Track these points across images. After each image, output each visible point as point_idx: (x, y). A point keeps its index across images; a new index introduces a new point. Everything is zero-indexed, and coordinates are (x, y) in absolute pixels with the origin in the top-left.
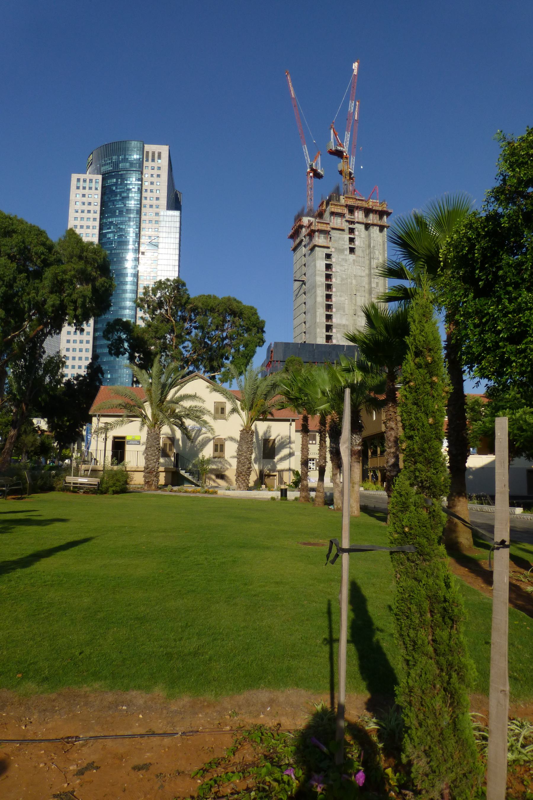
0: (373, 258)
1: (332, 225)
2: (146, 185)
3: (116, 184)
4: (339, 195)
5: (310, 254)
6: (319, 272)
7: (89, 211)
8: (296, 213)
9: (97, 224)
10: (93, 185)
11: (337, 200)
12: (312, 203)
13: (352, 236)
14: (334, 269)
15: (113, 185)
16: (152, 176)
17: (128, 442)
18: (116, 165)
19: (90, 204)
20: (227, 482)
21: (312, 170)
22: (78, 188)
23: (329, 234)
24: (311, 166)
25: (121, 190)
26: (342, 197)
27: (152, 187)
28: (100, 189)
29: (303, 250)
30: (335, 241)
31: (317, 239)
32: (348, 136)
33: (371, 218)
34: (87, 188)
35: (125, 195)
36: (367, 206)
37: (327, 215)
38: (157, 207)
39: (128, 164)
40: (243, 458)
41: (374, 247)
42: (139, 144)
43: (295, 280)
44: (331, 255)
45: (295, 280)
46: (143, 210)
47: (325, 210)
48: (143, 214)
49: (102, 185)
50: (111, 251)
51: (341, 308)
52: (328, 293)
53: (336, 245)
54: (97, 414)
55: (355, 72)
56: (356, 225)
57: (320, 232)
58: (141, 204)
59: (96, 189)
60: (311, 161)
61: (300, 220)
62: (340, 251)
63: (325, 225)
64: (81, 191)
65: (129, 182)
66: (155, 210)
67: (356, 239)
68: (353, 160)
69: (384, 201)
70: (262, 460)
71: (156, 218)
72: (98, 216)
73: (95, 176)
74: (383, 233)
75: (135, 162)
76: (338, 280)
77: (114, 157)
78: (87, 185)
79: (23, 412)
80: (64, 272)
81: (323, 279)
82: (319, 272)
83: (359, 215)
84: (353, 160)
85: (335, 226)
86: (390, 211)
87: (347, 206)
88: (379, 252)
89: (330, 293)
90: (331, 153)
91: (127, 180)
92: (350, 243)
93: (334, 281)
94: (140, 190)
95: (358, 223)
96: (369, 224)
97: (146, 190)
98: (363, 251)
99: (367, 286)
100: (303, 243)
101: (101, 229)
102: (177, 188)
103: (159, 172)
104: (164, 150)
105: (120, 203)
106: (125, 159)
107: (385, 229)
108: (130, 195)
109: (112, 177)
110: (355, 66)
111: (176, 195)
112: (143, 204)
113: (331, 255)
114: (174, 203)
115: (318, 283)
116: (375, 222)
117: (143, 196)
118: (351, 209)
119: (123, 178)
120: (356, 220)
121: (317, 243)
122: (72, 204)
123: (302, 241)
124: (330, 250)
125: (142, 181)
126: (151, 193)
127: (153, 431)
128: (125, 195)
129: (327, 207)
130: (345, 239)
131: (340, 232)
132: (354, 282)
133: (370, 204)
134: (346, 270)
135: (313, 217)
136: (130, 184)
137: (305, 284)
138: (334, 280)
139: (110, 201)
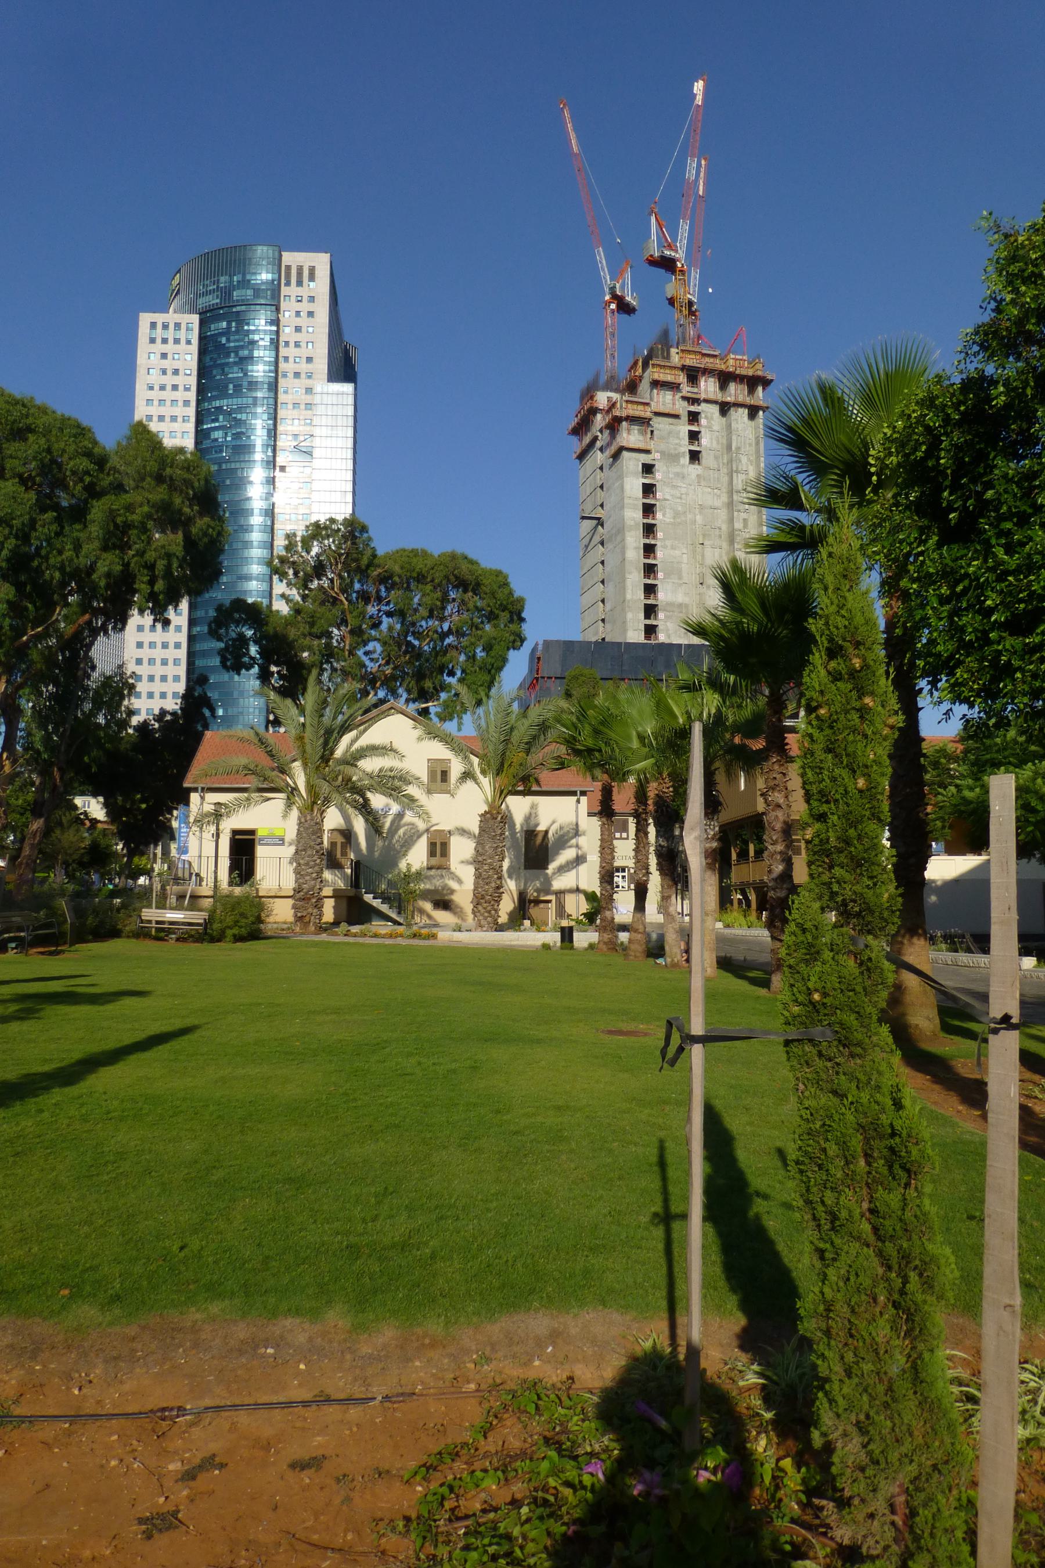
0: (737, 472)
1: (654, 407)
2: (287, 332)
3: (227, 332)
4: (669, 347)
5: (611, 466)
6: (631, 501)
7: (175, 387)
8: (583, 384)
9: (191, 411)
10: (182, 335)
11: (663, 357)
12: (614, 364)
13: (694, 428)
14: (659, 495)
15: (222, 334)
16: (298, 314)
17: (260, 840)
18: (226, 293)
19: (176, 372)
20: (455, 913)
21: (615, 297)
22: (152, 341)
23: (649, 425)
24: (612, 290)
25: (237, 344)
26: (673, 351)
27: (298, 337)
28: (195, 341)
29: (598, 457)
30: (662, 438)
31: (625, 435)
32: (684, 228)
33: (733, 392)
34: (171, 341)
35: (246, 352)
36: (723, 367)
37: (644, 386)
38: (309, 377)
39: (250, 292)
40: (486, 867)
41: (738, 448)
42: (271, 252)
43: (583, 518)
44: (653, 466)
45: (583, 518)
46: (282, 382)
47: (641, 378)
48: (281, 390)
49: (200, 334)
50: (220, 464)
51: (675, 571)
52: (648, 541)
53: (663, 446)
54: (200, 786)
55: (699, 100)
56: (703, 405)
57: (631, 421)
58: (276, 371)
59: (189, 342)
60: (611, 280)
61: (592, 398)
62: (672, 458)
63: (641, 407)
64: (159, 347)
65: (252, 328)
66: (304, 382)
67: (703, 433)
68: (695, 276)
69: (759, 357)
70: (523, 872)
71: (308, 399)
72: (192, 396)
73: (186, 315)
74: (757, 420)
75: (263, 287)
76: (668, 515)
77: (222, 279)
78: (170, 334)
79: (55, 786)
80: (130, 508)
81: (639, 514)
82: (631, 501)
83: (708, 387)
84: (695, 276)
85: (662, 409)
86: (769, 377)
87: (683, 368)
88: (749, 460)
89: (653, 542)
90: (653, 262)
91: (248, 324)
92: (691, 443)
94: (275, 344)
95: (707, 401)
96: (727, 403)
97: (287, 344)
98: (716, 458)
99: (724, 527)
100: (598, 444)
101: (199, 422)
102: (349, 337)
103: (311, 307)
104: (321, 262)
105: (236, 369)
106: (244, 280)
107: (761, 413)
108: (256, 354)
109: (219, 318)
110: (699, 87)
111: (346, 352)
112: (280, 370)
113: (653, 466)
114: (343, 367)
115: (629, 523)
116: (741, 399)
117: (281, 354)
118: (693, 375)
119: (241, 320)
120: (703, 396)
121: (625, 444)
122: (141, 372)
123: (596, 438)
124: (651, 456)
125: (278, 326)
126: (297, 349)
127: (309, 817)
128: (246, 352)
129: (644, 371)
130: (681, 434)
131: (671, 420)
132: (698, 517)
133: (731, 364)
134: (684, 496)
135: (616, 391)
136: (254, 332)
137: (602, 525)
138: (659, 515)
139: (216, 366)
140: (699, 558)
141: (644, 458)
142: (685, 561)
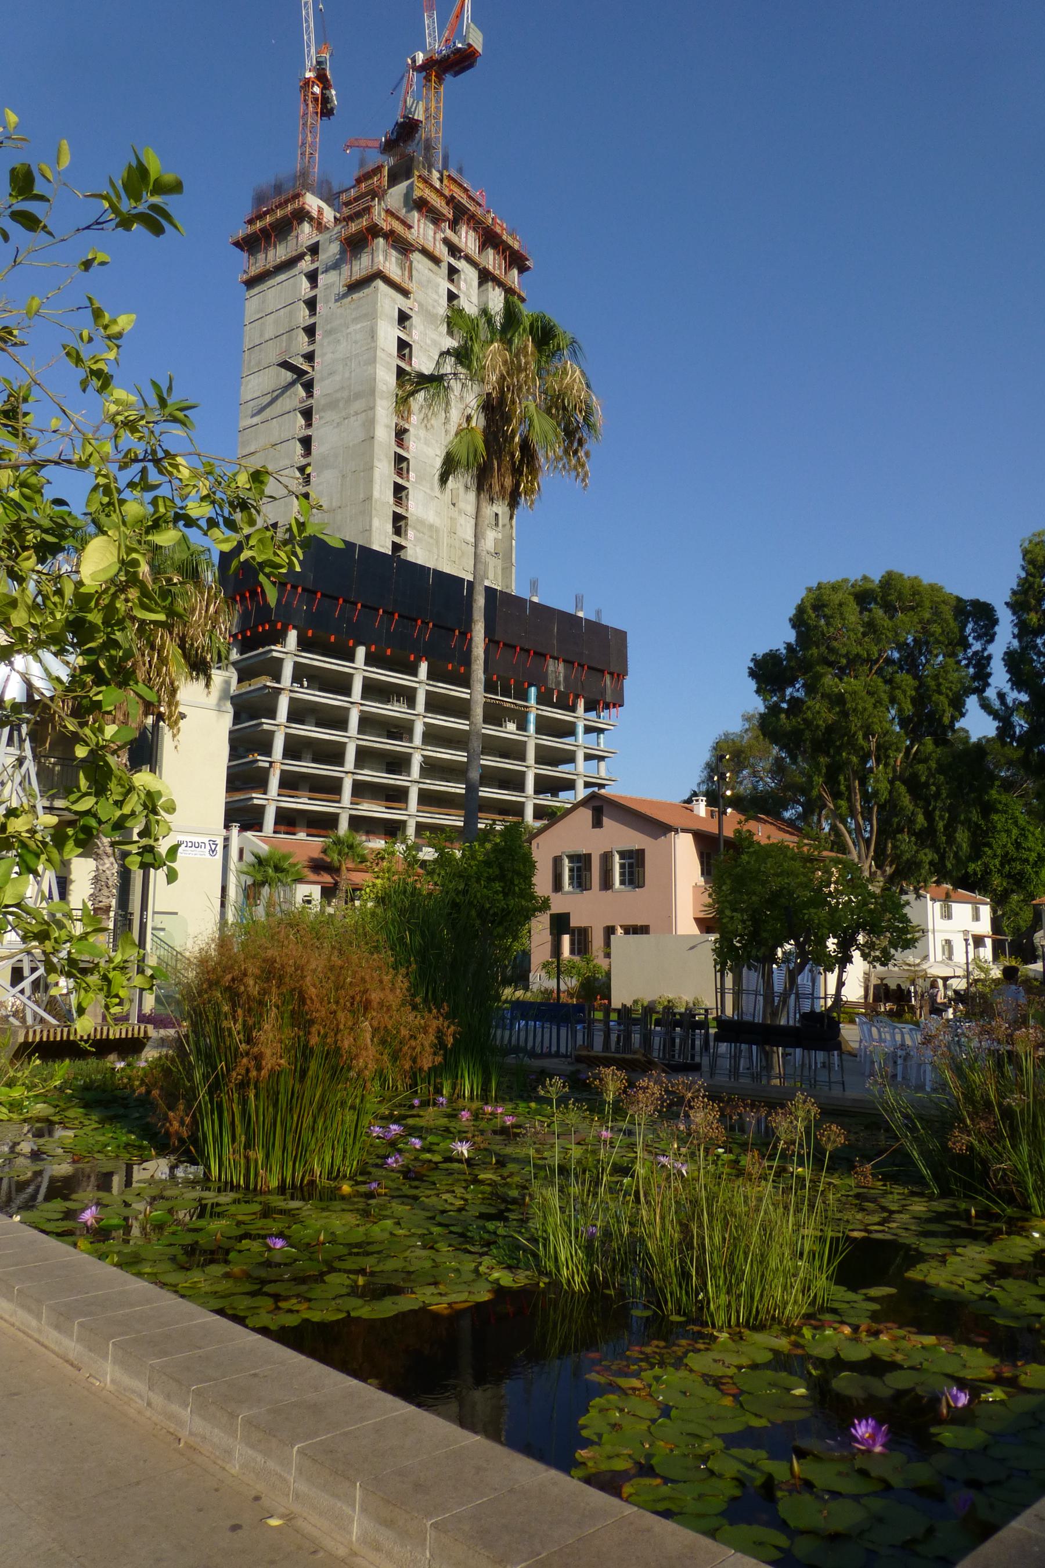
83: (467, 239)
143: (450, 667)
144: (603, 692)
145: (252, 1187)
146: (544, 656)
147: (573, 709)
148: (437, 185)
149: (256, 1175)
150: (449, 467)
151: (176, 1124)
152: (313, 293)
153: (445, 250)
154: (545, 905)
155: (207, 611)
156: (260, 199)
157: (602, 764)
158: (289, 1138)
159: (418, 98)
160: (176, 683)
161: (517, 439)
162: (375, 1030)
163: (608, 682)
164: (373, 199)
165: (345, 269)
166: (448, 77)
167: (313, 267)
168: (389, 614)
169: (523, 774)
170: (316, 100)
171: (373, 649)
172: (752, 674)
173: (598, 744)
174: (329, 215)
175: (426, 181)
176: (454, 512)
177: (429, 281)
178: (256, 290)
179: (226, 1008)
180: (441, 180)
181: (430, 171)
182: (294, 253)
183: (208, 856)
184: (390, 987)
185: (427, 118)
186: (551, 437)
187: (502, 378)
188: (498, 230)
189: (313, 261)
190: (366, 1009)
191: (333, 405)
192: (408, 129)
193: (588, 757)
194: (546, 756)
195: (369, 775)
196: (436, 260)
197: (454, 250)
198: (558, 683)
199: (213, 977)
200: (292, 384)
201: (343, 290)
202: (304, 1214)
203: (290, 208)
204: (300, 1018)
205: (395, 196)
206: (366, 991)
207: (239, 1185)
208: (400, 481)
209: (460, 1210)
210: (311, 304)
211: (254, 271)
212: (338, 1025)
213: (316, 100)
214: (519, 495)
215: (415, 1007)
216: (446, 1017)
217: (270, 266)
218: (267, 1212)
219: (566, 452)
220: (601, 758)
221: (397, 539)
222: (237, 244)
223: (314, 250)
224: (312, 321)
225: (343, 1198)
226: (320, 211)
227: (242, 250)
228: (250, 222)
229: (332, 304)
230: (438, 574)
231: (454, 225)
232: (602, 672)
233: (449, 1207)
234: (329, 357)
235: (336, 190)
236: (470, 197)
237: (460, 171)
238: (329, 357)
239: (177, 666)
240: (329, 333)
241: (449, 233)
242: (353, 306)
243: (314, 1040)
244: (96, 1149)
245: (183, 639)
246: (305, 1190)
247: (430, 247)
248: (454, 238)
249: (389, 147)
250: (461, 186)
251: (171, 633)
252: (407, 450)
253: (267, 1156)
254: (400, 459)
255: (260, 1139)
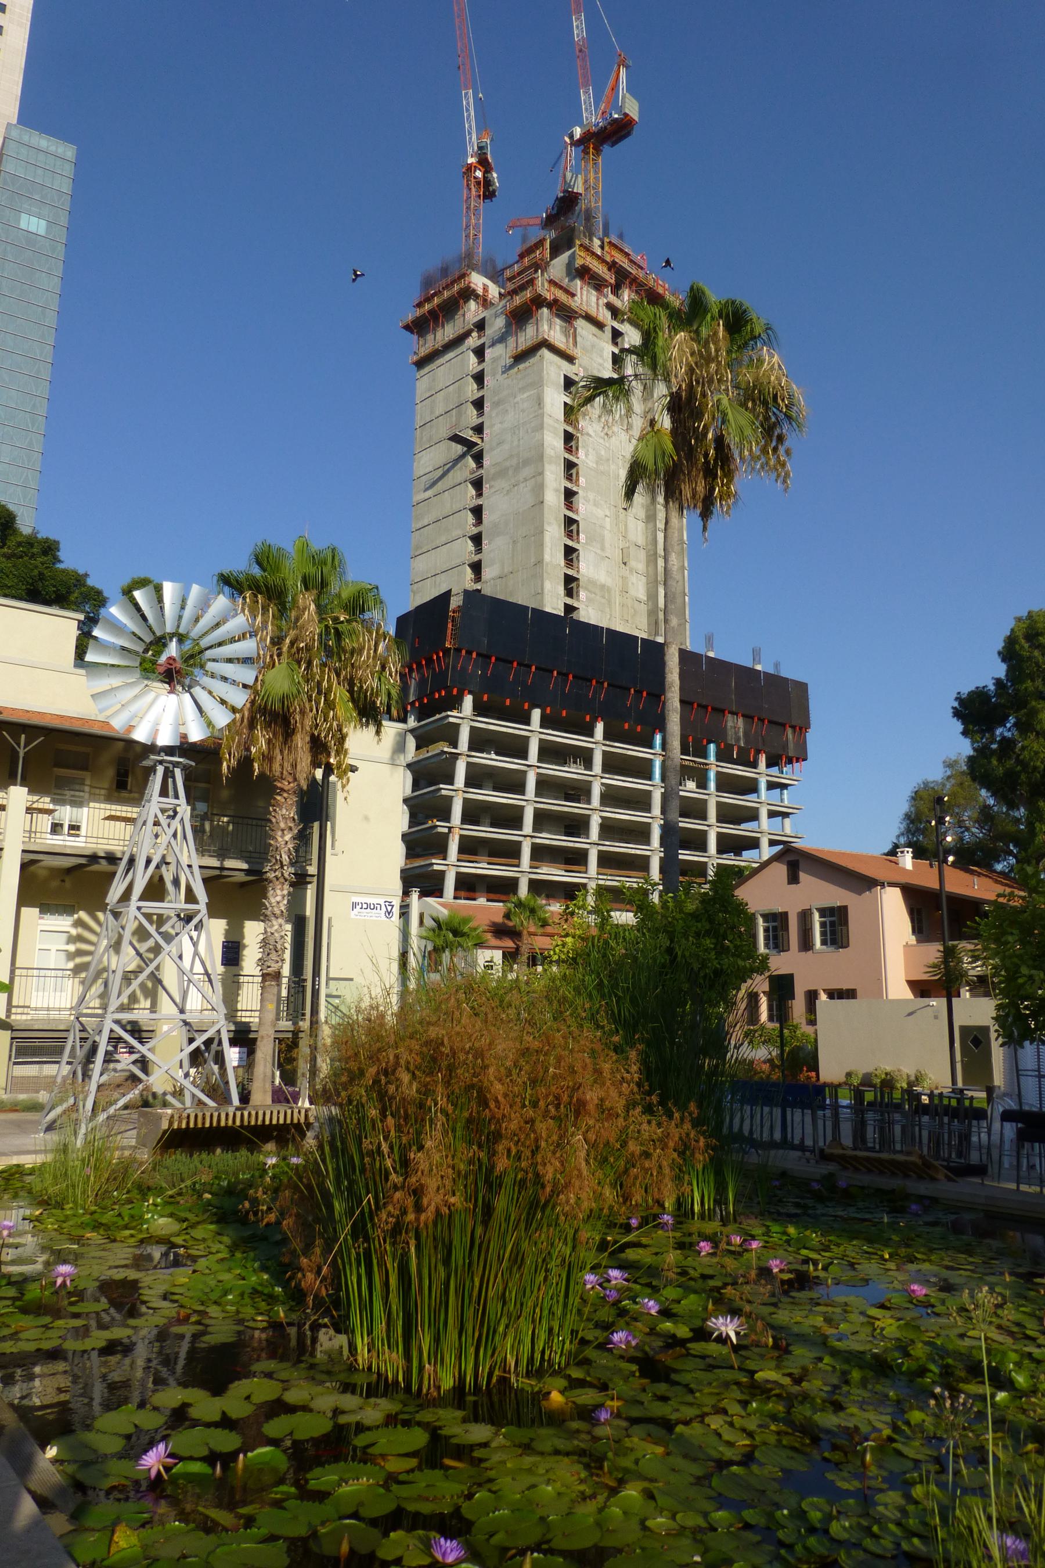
52: (569, 485)
81: (560, 443)
93: (584, 458)
115: (549, 452)
140: (622, 527)
141: (566, 368)
142: (608, 527)
143: (626, 726)
144: (785, 746)
145: (415, 1387)
146: (723, 711)
147: (754, 765)
148: (599, 252)
149: (421, 1368)
150: (636, 473)
151: (310, 1276)
152: (480, 368)
153: (608, 314)
154: (763, 965)
155: (376, 651)
156: (428, 282)
157: (787, 821)
158: (469, 1313)
159: (576, 172)
160: (345, 730)
161: (710, 436)
162: (593, 1145)
163: (790, 736)
164: (536, 271)
165: (511, 341)
166: (606, 148)
167: (480, 342)
168: (563, 675)
169: (704, 835)
170: (478, 183)
171: (548, 710)
172: (957, 714)
173: (782, 800)
174: (494, 291)
175: (588, 249)
176: (625, 571)
177: (593, 346)
178: (427, 369)
179: (373, 1113)
180: (602, 247)
181: (591, 240)
182: (461, 331)
183: (384, 918)
184: (611, 1081)
185: (586, 189)
186: (748, 432)
187: (691, 371)
188: (660, 291)
189: (479, 337)
190: (578, 1113)
191: (502, 473)
192: (568, 202)
193: (772, 814)
194: (727, 814)
195: (547, 838)
196: (600, 325)
197: (615, 312)
198: (738, 739)
199: (353, 1065)
200: (463, 456)
201: (509, 361)
202: (496, 1458)
203: (456, 288)
204: (482, 1131)
205: (558, 267)
206: (577, 1087)
207: (396, 1382)
208: (570, 543)
209: (748, 1459)
210: (479, 378)
211: (423, 352)
212: (537, 1140)
213: (478, 183)
214: (713, 504)
215: (649, 1110)
216: (696, 1123)
217: (438, 345)
218: (437, 1452)
219: (764, 451)
220: (785, 815)
221: (569, 601)
222: (407, 328)
223: (480, 326)
224: (480, 394)
225: (555, 1419)
226: (485, 288)
227: (412, 332)
228: (419, 305)
229: (499, 376)
230: (611, 633)
231: (616, 290)
232: (783, 725)
233: (729, 1454)
234: (497, 428)
235: (500, 266)
236: (631, 261)
237: (621, 236)
238: (497, 428)
239: (344, 708)
240: (496, 404)
241: (612, 298)
242: (519, 376)
243: (502, 1163)
244: (214, 1296)
245: (351, 683)
246: (494, 1401)
247: (593, 312)
248: (618, 303)
249: (550, 221)
250: (621, 251)
251: (338, 675)
252: (577, 512)
253: (437, 1340)
254: (569, 522)
255: (423, 1316)
